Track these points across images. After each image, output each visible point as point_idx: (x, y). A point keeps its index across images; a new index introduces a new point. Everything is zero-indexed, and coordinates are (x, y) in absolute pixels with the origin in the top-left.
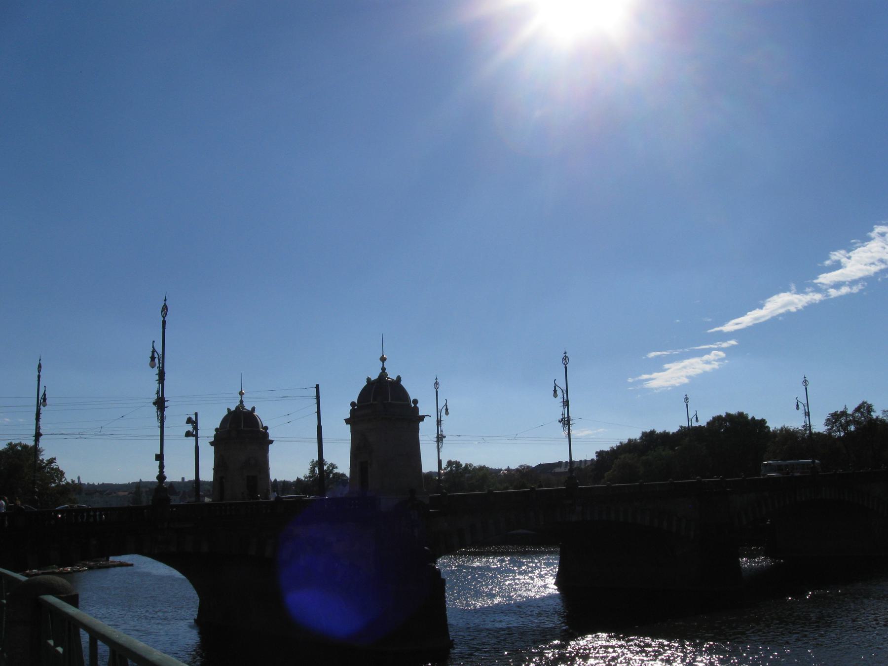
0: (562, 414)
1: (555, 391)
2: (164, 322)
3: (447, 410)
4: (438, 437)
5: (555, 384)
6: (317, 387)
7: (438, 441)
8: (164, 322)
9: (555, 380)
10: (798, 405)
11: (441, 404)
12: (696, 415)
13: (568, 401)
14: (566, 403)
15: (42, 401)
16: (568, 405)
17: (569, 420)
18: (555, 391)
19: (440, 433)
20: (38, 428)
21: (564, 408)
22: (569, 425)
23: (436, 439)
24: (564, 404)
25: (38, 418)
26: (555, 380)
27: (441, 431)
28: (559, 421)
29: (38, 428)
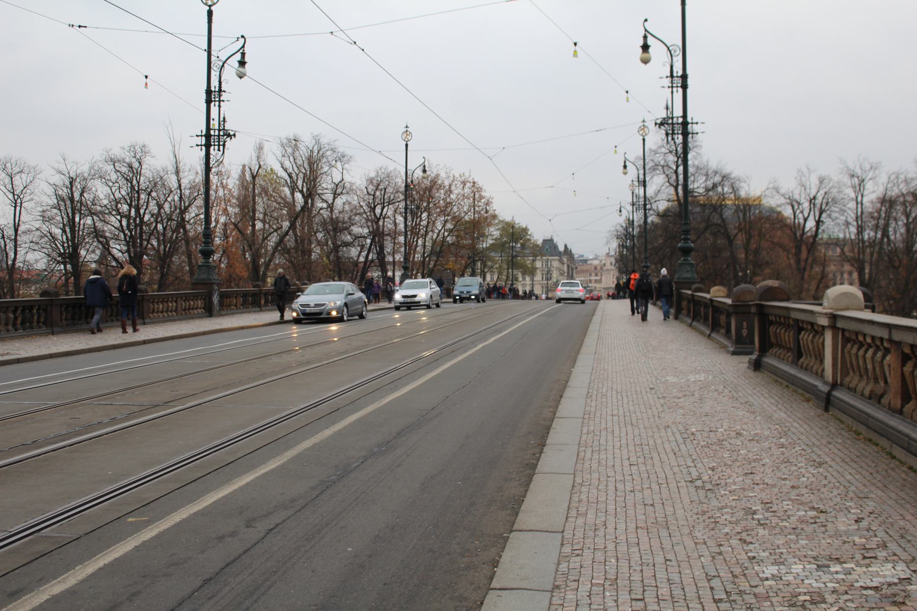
0: (667, 108)
1: (645, 48)
3: (242, 63)
4: (208, 136)
5: (646, 30)
7: (208, 146)
9: (646, 20)
11: (223, 47)
13: (684, 77)
14: (678, 82)
16: (684, 87)
17: (685, 124)
18: (645, 48)
19: (215, 124)
21: (672, 92)
22: (685, 134)
26: (646, 20)
28: (656, 124)
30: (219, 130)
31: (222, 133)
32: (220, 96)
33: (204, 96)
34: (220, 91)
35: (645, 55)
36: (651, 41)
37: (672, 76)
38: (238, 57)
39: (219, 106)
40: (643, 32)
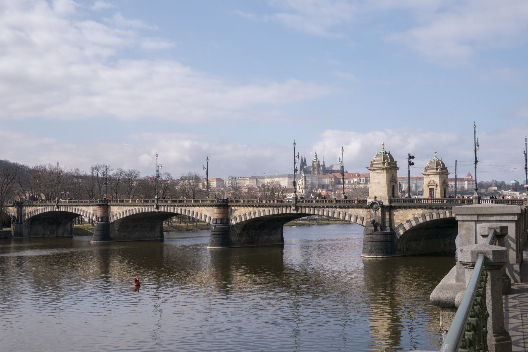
2: (526, 144)
4: (295, 170)
6: (456, 161)
7: (295, 172)
8: (526, 144)
10: (204, 169)
12: (161, 164)
13: (343, 167)
15: (477, 145)
20: (476, 157)
22: (343, 176)
23: (294, 171)
25: (476, 153)
27: (296, 168)
29: (476, 157)
33: (294, 163)
38: (298, 156)
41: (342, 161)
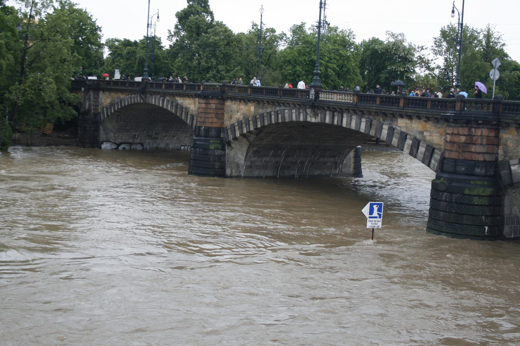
1: (453, 12)
14: (460, 25)
18: (453, 12)
19: (322, 18)
24: (459, 25)
30: (324, 21)
31: (325, 22)
32: (325, 6)
34: (325, 4)
35: (453, 14)
36: (455, 9)
37: (459, 23)
39: (324, 10)
40: (453, 6)
41: (461, 11)
